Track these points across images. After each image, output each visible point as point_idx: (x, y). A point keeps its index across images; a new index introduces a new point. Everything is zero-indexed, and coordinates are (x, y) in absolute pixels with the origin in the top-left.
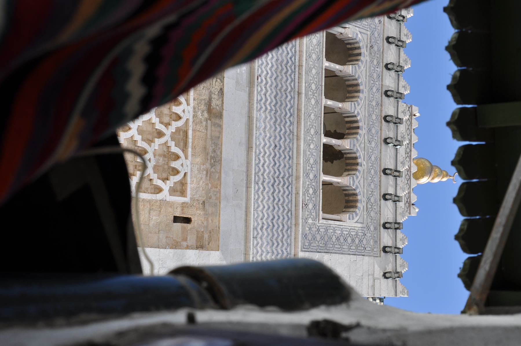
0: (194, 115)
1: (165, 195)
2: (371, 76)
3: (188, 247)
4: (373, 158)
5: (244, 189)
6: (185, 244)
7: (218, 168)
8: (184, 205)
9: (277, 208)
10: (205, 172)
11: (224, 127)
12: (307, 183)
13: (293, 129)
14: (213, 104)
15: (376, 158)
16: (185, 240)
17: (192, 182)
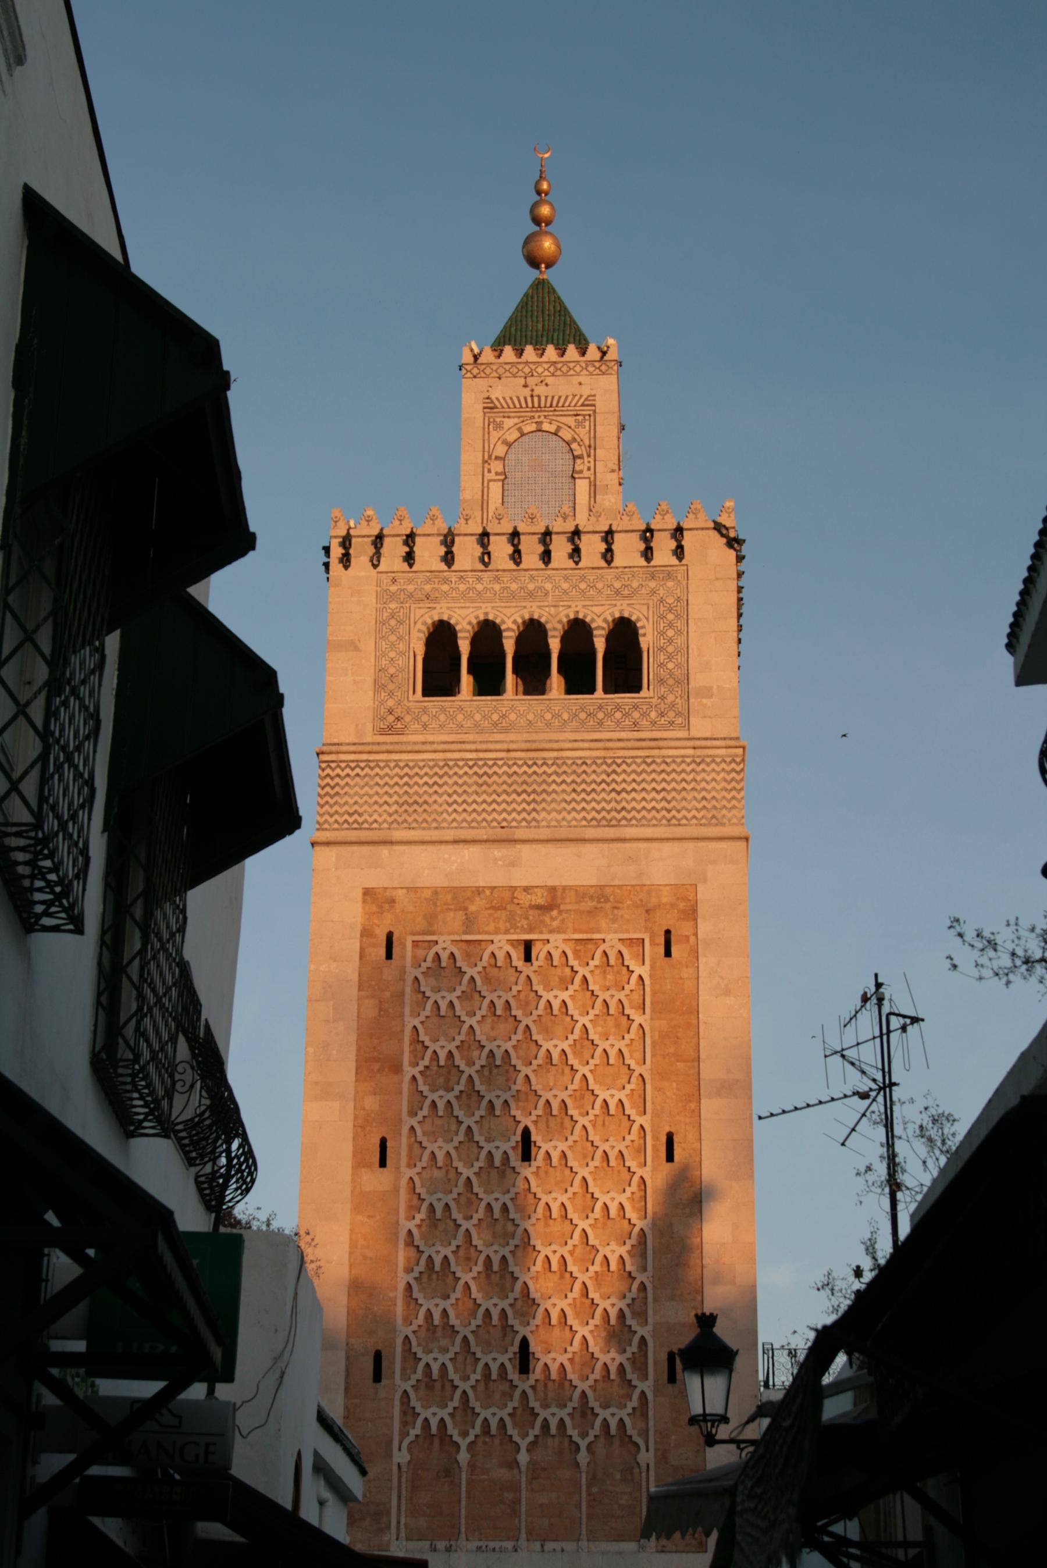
0: (559, 932)
1: (644, 971)
2: (464, 596)
3: (696, 935)
4: (565, 586)
5: (628, 845)
6: (692, 939)
7: (608, 890)
8: (653, 943)
9: (644, 785)
10: (616, 911)
11: (564, 884)
12: (609, 723)
13: (550, 759)
14: (541, 901)
15: (566, 578)
16: (688, 937)
17: (627, 931)
